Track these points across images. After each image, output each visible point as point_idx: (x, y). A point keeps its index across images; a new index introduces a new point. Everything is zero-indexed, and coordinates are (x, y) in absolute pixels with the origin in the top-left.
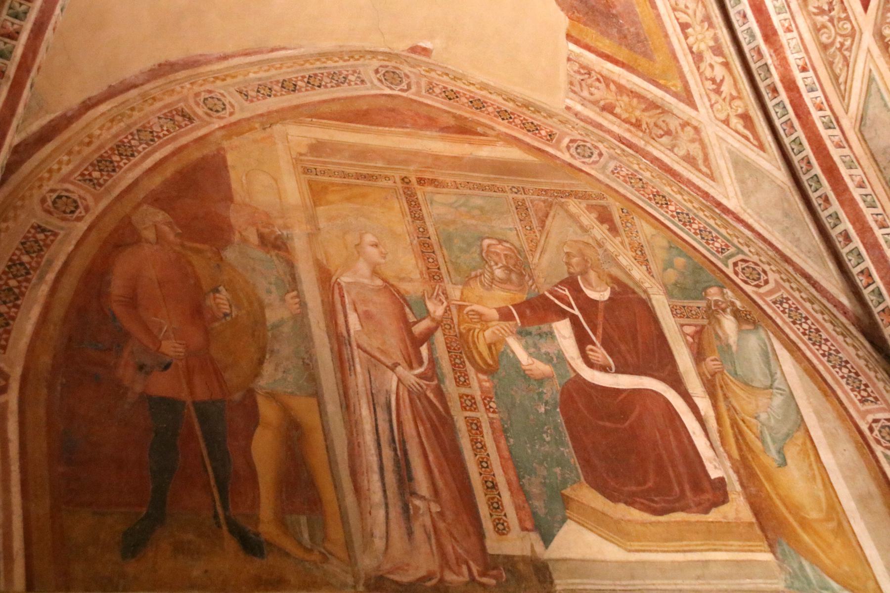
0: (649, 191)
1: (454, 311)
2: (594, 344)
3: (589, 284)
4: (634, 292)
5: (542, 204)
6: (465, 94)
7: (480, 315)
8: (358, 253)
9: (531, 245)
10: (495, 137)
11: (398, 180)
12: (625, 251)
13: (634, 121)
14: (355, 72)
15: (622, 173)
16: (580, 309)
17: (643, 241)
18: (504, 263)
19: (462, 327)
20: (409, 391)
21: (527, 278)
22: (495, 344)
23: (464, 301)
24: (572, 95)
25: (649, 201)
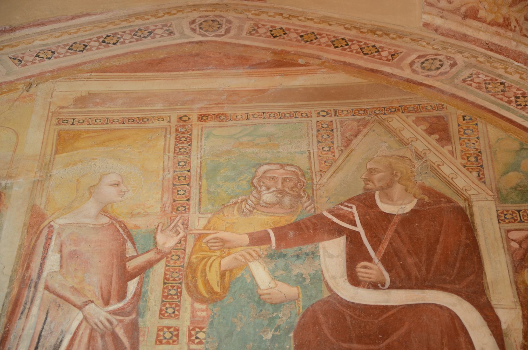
0: (511, 94)
1: (191, 240)
2: (370, 260)
3: (388, 198)
4: (449, 201)
5: (355, 124)
6: (295, 30)
7: (223, 241)
8: (91, 193)
9: (323, 165)
10: (318, 65)
11: (174, 119)
12: (453, 160)
13: (501, 21)
14: (166, 25)
15: (476, 80)
16: (365, 225)
17: (482, 148)
18: (280, 186)
19: (194, 257)
20: (92, 330)
21: (304, 199)
22: (231, 271)
23: (209, 230)
24: (428, 9)
25: (507, 105)
